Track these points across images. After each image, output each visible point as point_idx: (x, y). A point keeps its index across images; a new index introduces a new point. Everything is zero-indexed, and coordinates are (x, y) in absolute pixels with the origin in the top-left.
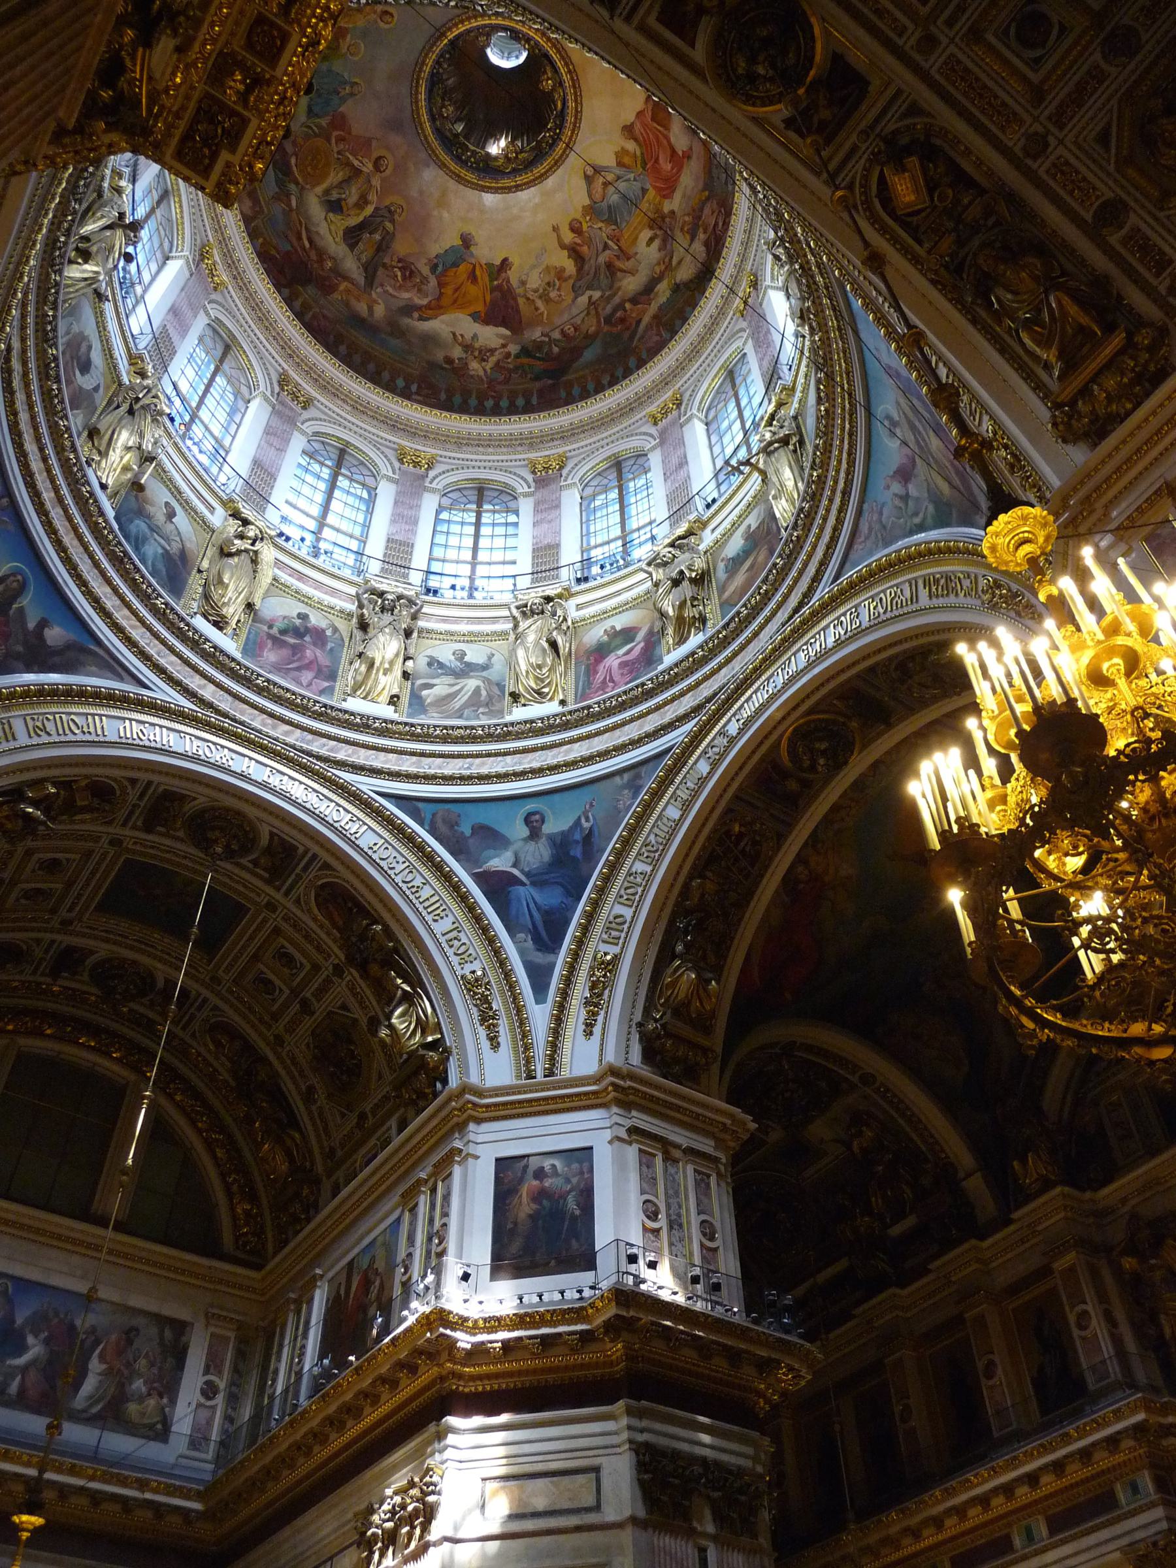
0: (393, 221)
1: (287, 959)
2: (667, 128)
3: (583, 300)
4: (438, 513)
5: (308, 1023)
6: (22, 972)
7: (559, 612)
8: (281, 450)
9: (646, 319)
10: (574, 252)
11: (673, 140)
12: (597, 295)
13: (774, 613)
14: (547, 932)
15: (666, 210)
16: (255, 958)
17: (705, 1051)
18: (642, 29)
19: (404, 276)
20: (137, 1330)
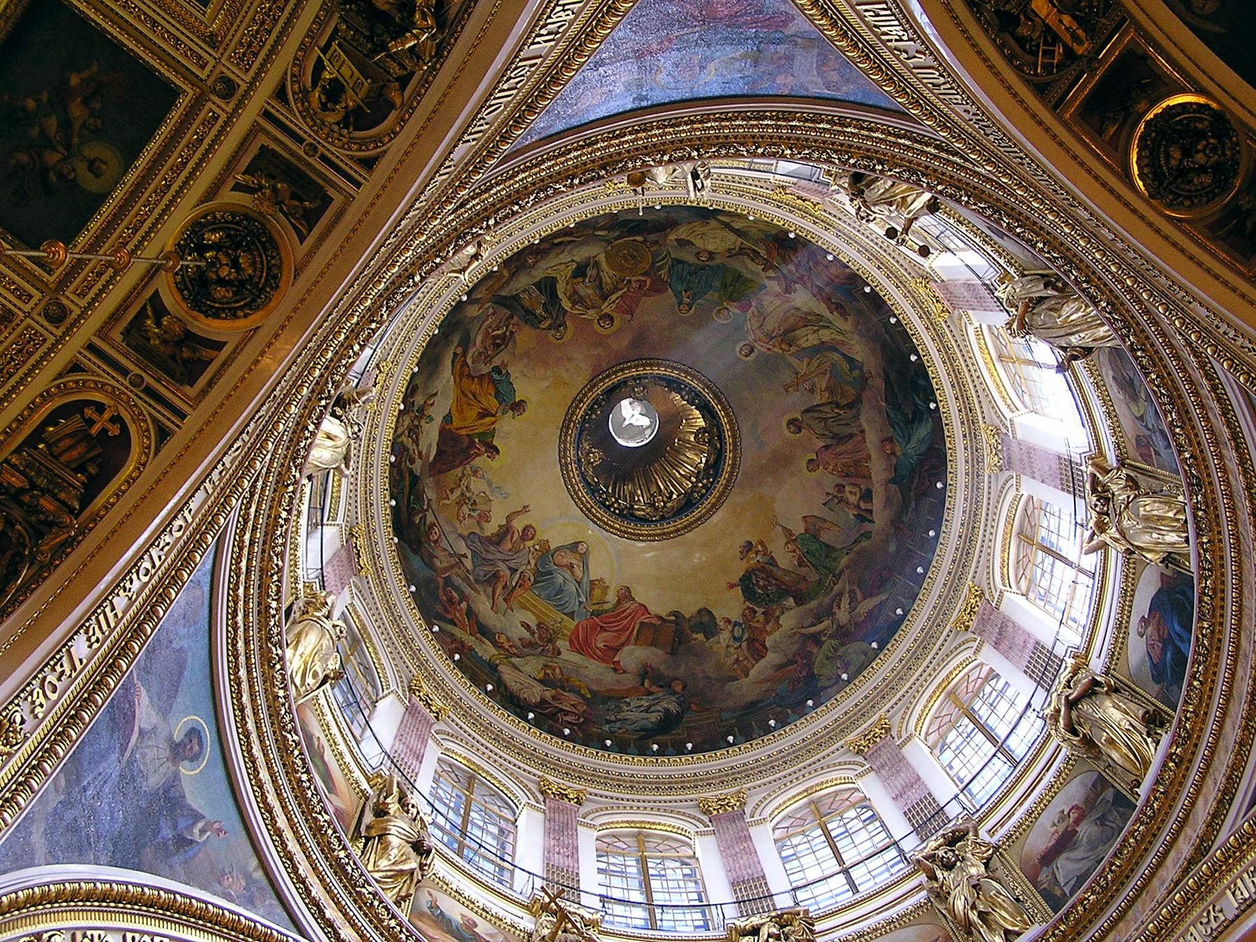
0: (549, 328)
3: (462, 548)
9: (457, 632)
10: (505, 531)
11: (626, 648)
12: (468, 563)
15: (559, 643)
19: (498, 337)
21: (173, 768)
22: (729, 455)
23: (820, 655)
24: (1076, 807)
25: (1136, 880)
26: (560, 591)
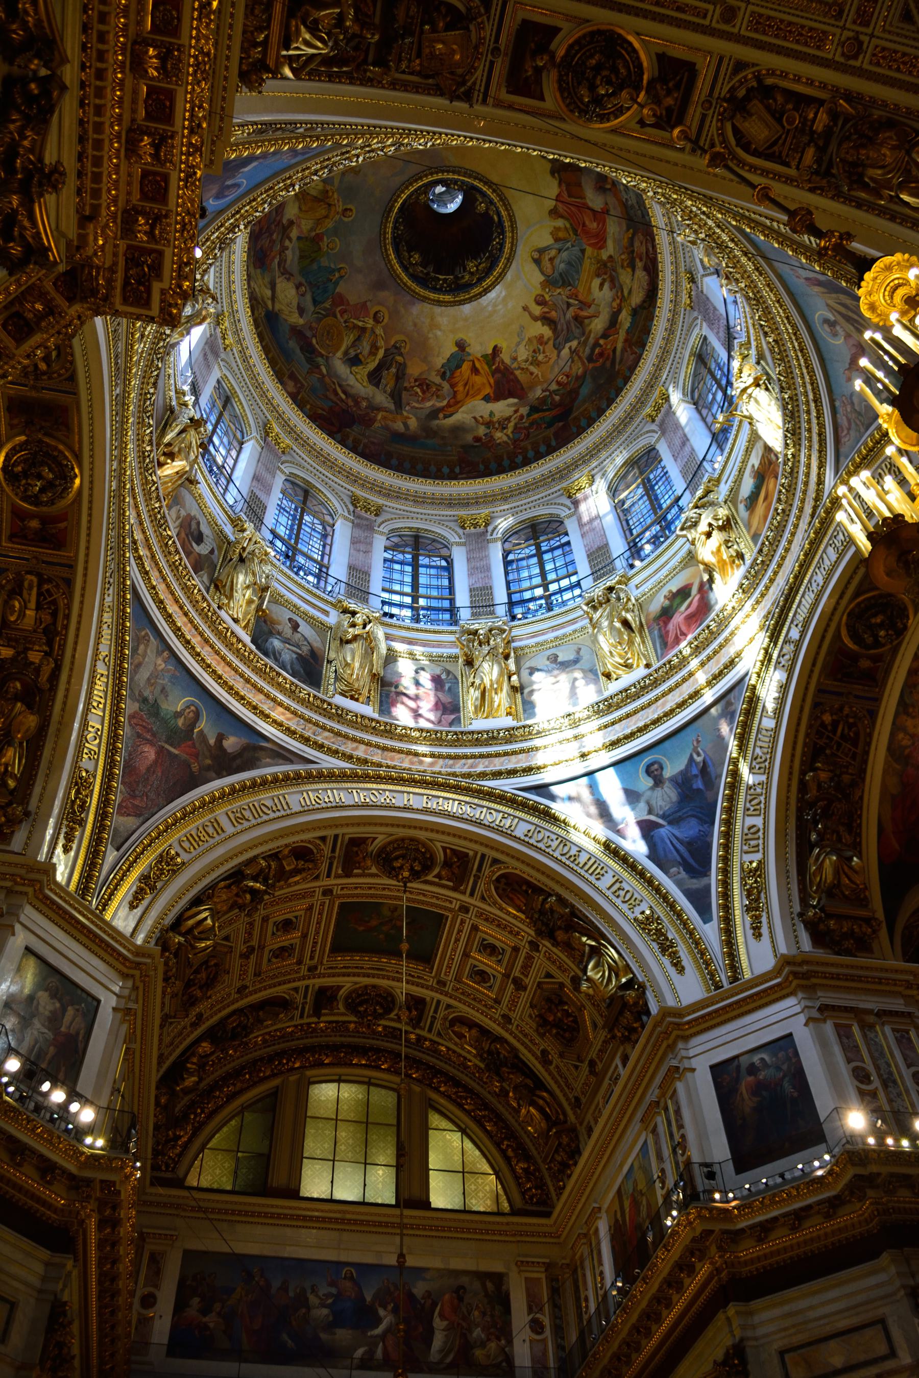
0: (401, 354)
1: (490, 949)
2: (584, 198)
3: (565, 352)
4: (505, 557)
5: (524, 998)
6: (292, 1019)
7: (622, 595)
8: (367, 552)
11: (590, 204)
12: (574, 344)
13: (796, 526)
14: (693, 859)
15: (605, 257)
16: (466, 955)
17: (868, 921)
18: (499, 104)
20: (462, 1287)
21: (667, 784)
26: (569, 263)
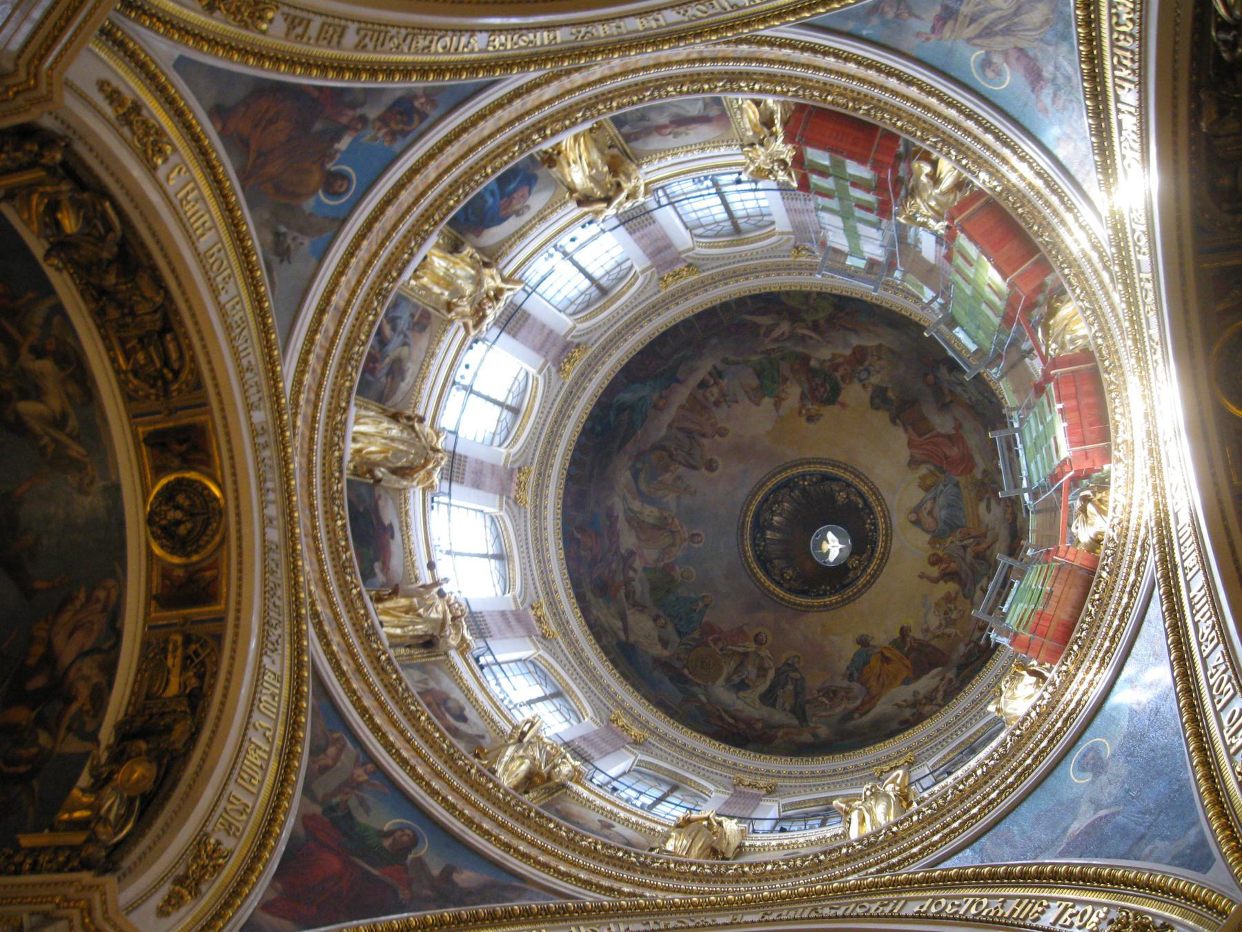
0: (796, 670)
10: (948, 576)
11: (942, 431)
15: (979, 476)
22: (770, 485)
23: (821, 316)
24: (660, 134)
25: (631, 79)
26: (950, 506)
